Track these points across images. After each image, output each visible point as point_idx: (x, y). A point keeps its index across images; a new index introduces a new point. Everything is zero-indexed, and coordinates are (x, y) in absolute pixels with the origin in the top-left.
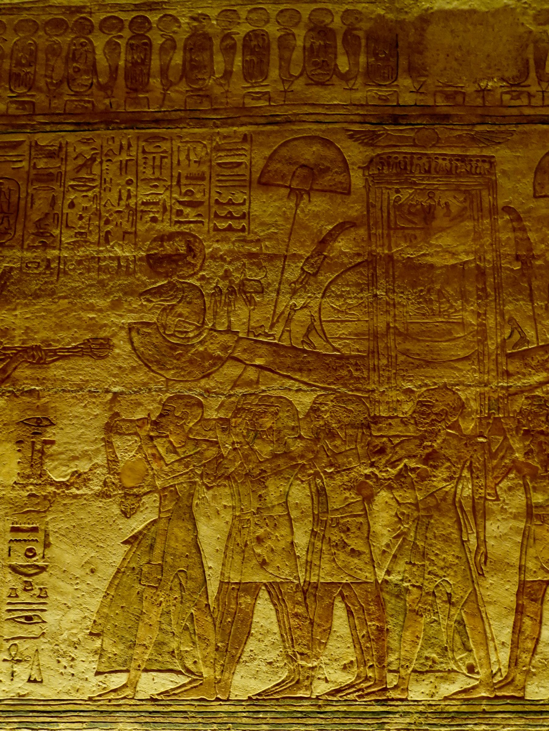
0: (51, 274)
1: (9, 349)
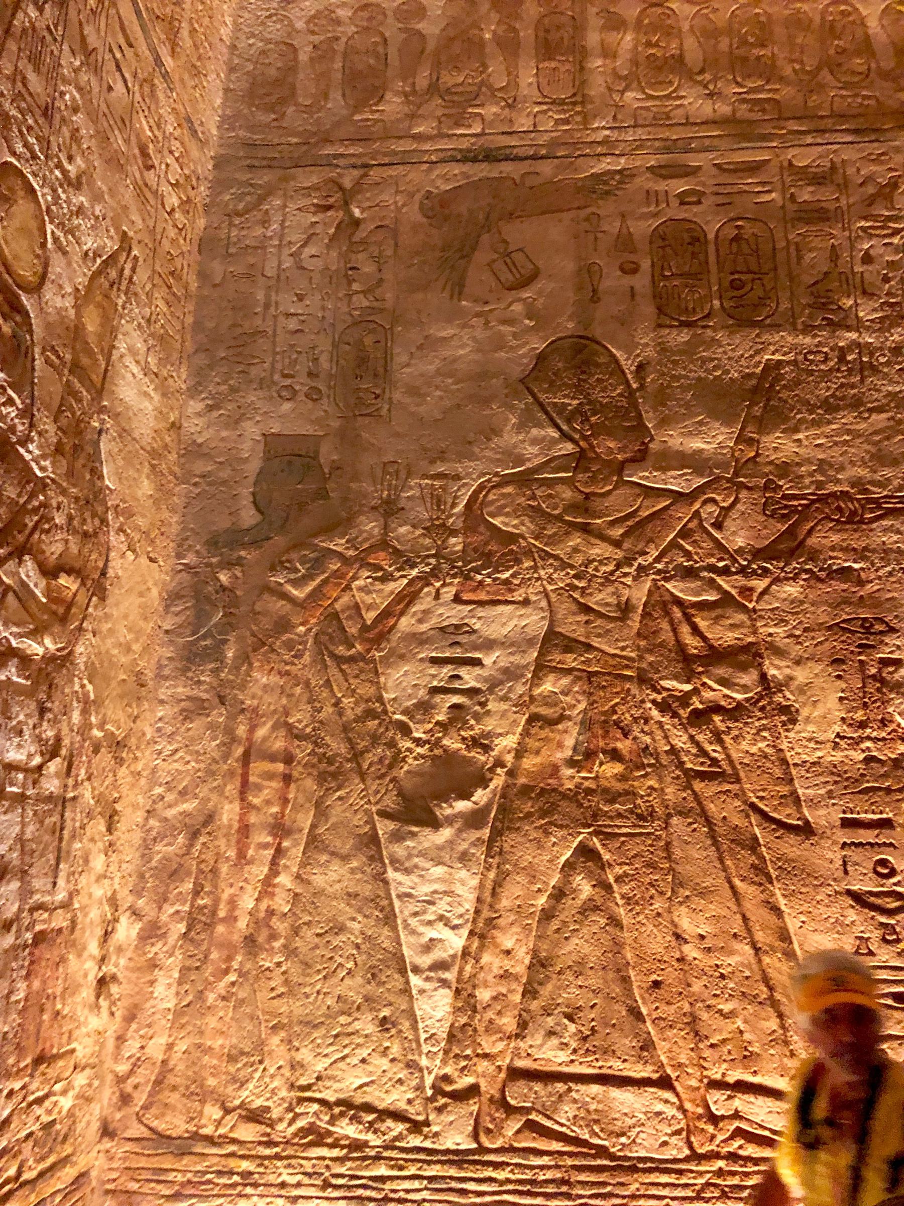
0: (850, 370)
1: (794, 497)
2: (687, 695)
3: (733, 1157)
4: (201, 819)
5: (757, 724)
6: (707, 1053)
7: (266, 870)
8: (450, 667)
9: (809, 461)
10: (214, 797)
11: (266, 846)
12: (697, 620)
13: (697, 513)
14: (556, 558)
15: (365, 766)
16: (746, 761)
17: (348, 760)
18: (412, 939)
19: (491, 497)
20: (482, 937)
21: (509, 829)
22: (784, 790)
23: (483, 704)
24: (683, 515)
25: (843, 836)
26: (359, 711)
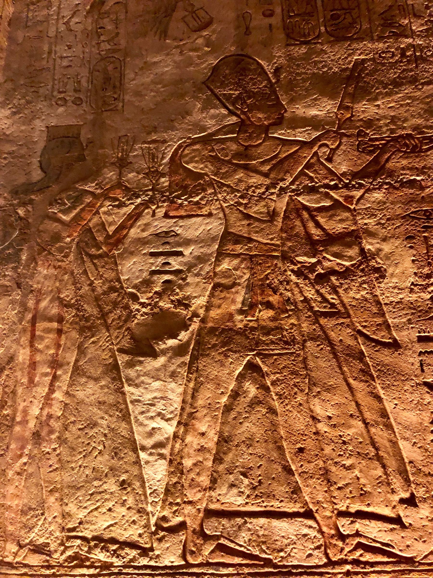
1: (377, 139)
2: (314, 265)
3: (356, 562)
4: (6, 360)
5: (359, 280)
6: (336, 494)
7: (46, 390)
8: (163, 257)
9: (385, 117)
10: (14, 346)
11: (46, 375)
12: (319, 218)
13: (316, 153)
14: (228, 186)
16: (353, 304)
17: (98, 319)
18: (140, 429)
19: (186, 152)
20: (186, 425)
21: (202, 355)
22: (379, 320)
23: (184, 279)
24: (307, 155)
25: (419, 348)
26: (105, 288)
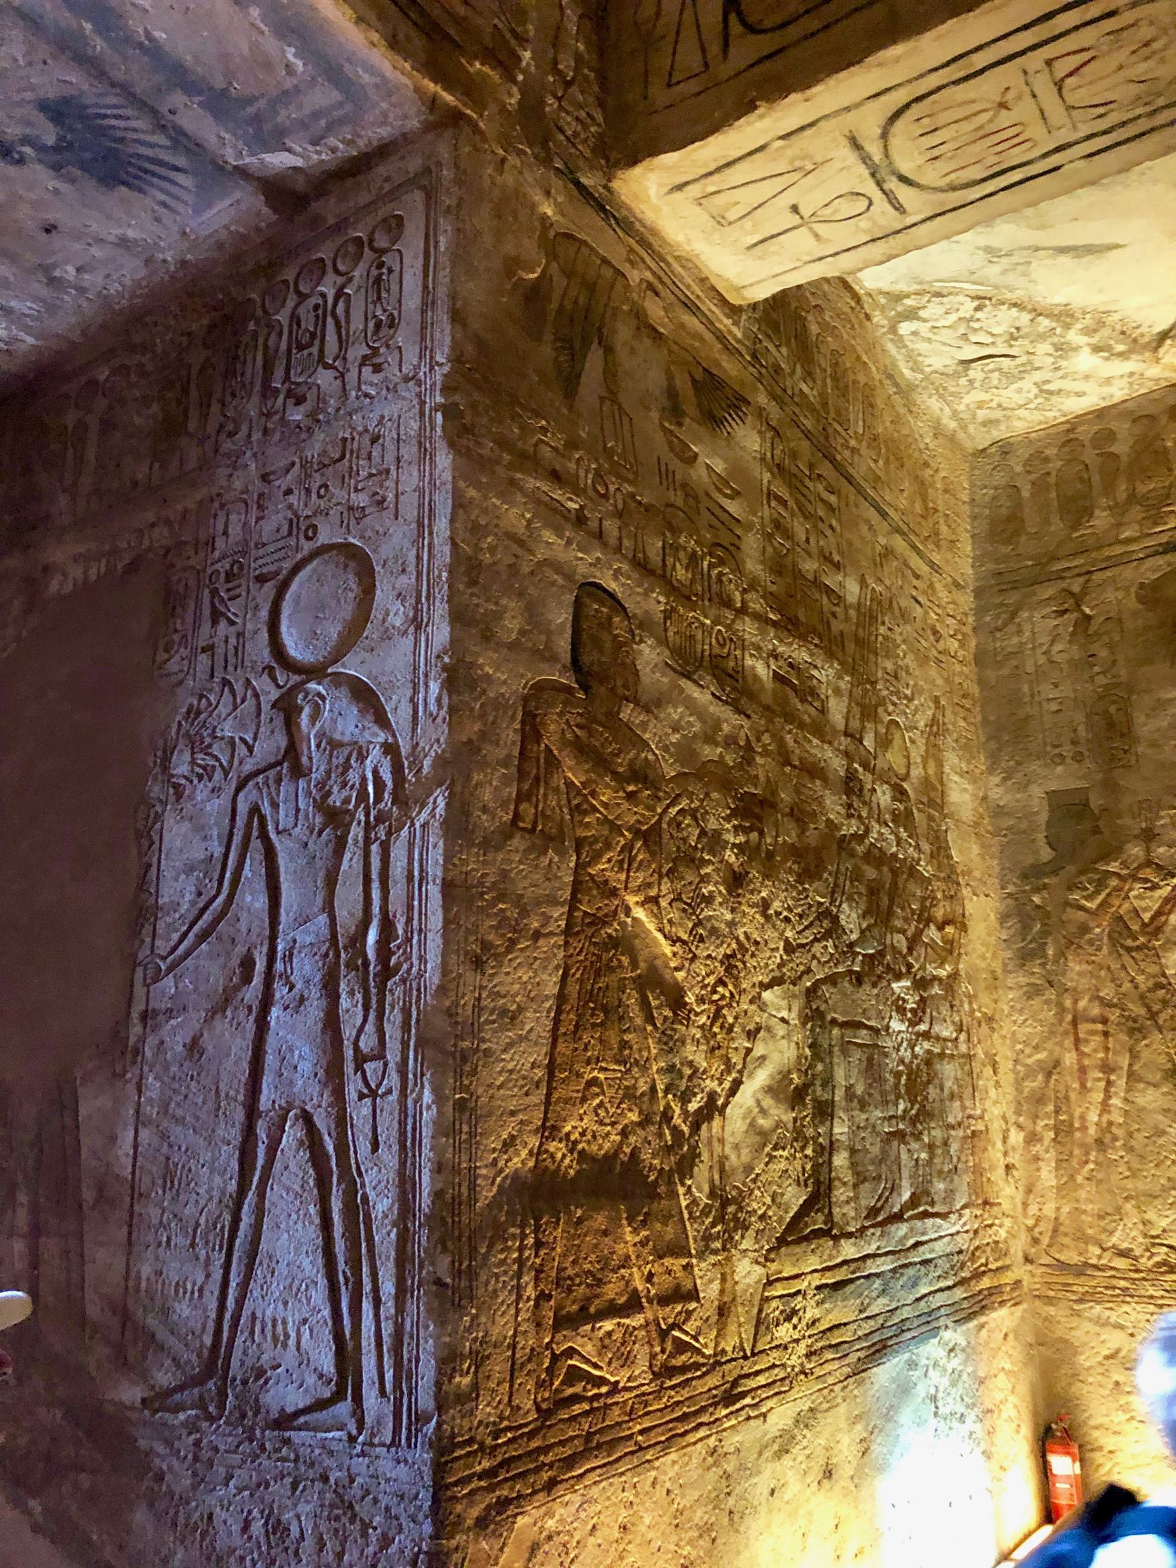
4: (1051, 1064)
10: (1057, 1048)
11: (1099, 1080)
15: (1161, 1022)
26: (1150, 984)
